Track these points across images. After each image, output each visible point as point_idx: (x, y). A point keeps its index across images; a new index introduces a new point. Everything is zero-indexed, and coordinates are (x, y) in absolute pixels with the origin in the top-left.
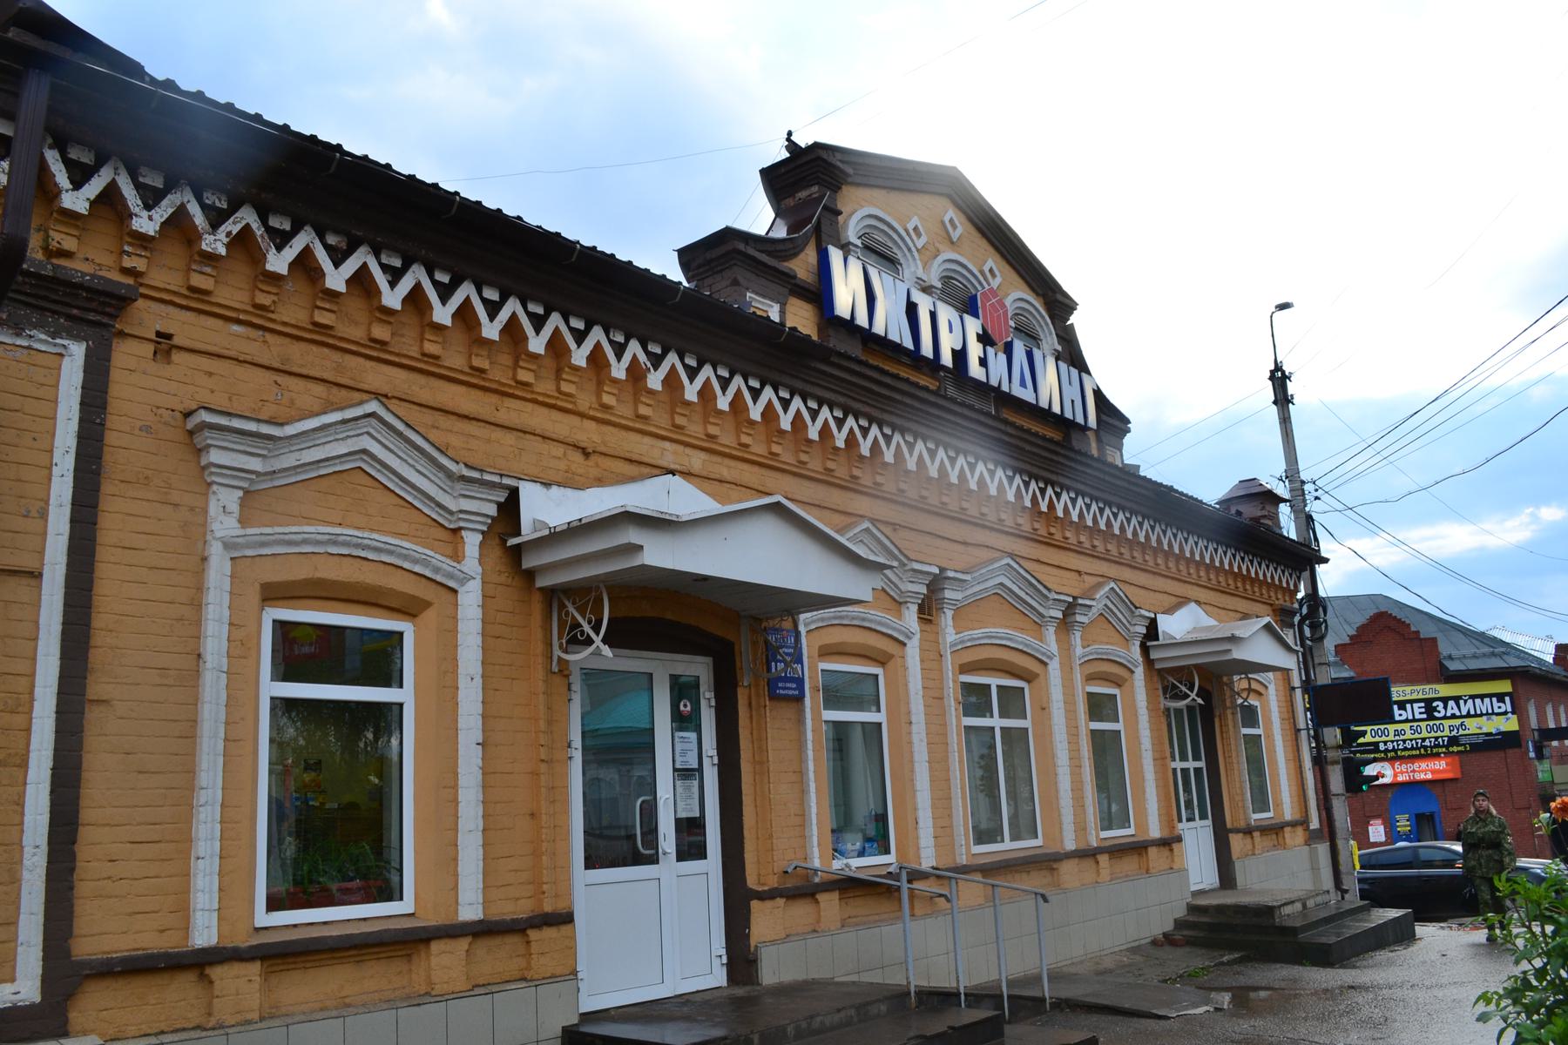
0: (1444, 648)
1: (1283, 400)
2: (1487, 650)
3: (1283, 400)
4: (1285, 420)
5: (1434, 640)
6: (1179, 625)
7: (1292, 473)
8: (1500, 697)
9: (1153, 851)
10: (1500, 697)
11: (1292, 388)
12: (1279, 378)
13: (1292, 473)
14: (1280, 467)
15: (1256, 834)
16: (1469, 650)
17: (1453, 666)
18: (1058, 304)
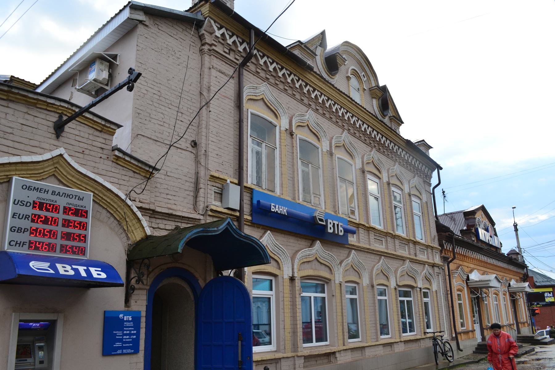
0: (535, 279)
1: (516, 230)
2: (546, 280)
3: (516, 230)
4: (517, 235)
5: (532, 277)
6: (513, 283)
7: (519, 247)
8: (550, 292)
9: (470, 333)
10: (550, 292)
11: (518, 227)
12: (515, 226)
13: (519, 247)
14: (516, 245)
15: (462, 334)
16: (541, 280)
17: (538, 284)
18: (493, 223)
